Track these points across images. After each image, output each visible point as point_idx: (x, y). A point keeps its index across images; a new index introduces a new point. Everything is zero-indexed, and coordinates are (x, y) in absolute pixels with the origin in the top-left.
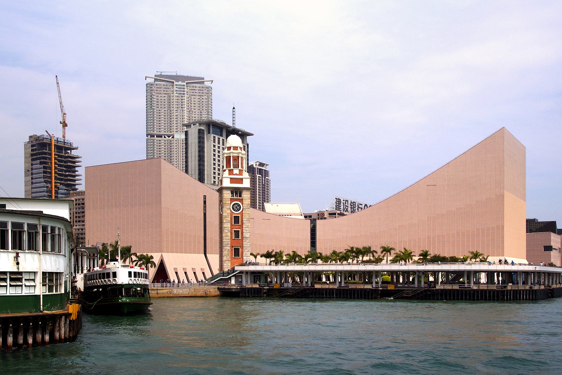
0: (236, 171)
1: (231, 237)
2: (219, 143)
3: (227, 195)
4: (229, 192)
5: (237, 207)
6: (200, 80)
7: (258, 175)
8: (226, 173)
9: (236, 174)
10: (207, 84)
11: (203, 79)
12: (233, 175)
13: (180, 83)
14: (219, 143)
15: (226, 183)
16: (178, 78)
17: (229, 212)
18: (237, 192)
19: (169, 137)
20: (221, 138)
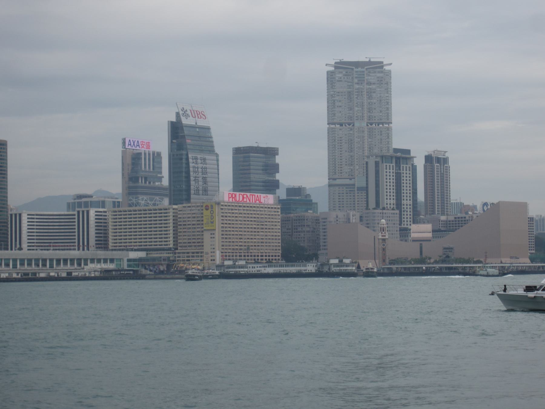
3: (381, 241)
5: (384, 245)
7: (436, 165)
8: (380, 234)
10: (387, 68)
11: (382, 62)
13: (360, 69)
15: (380, 237)
16: (357, 64)
18: (384, 240)
19: (349, 125)
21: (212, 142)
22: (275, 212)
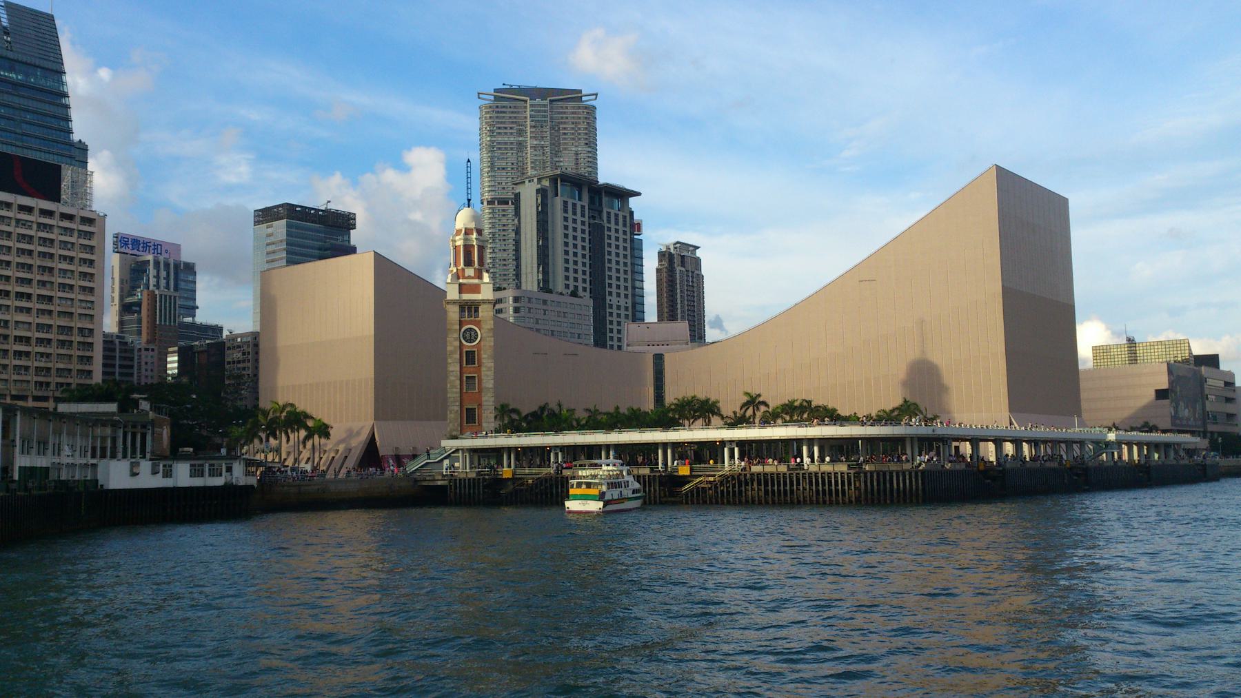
0: (470, 271)
1: (461, 389)
2: (575, 213)
4: (456, 309)
6: (574, 96)
9: (469, 277)
11: (580, 91)
12: (464, 278)
14: (575, 213)
17: (457, 343)
20: (579, 204)
21: (68, 107)
22: (42, 227)
